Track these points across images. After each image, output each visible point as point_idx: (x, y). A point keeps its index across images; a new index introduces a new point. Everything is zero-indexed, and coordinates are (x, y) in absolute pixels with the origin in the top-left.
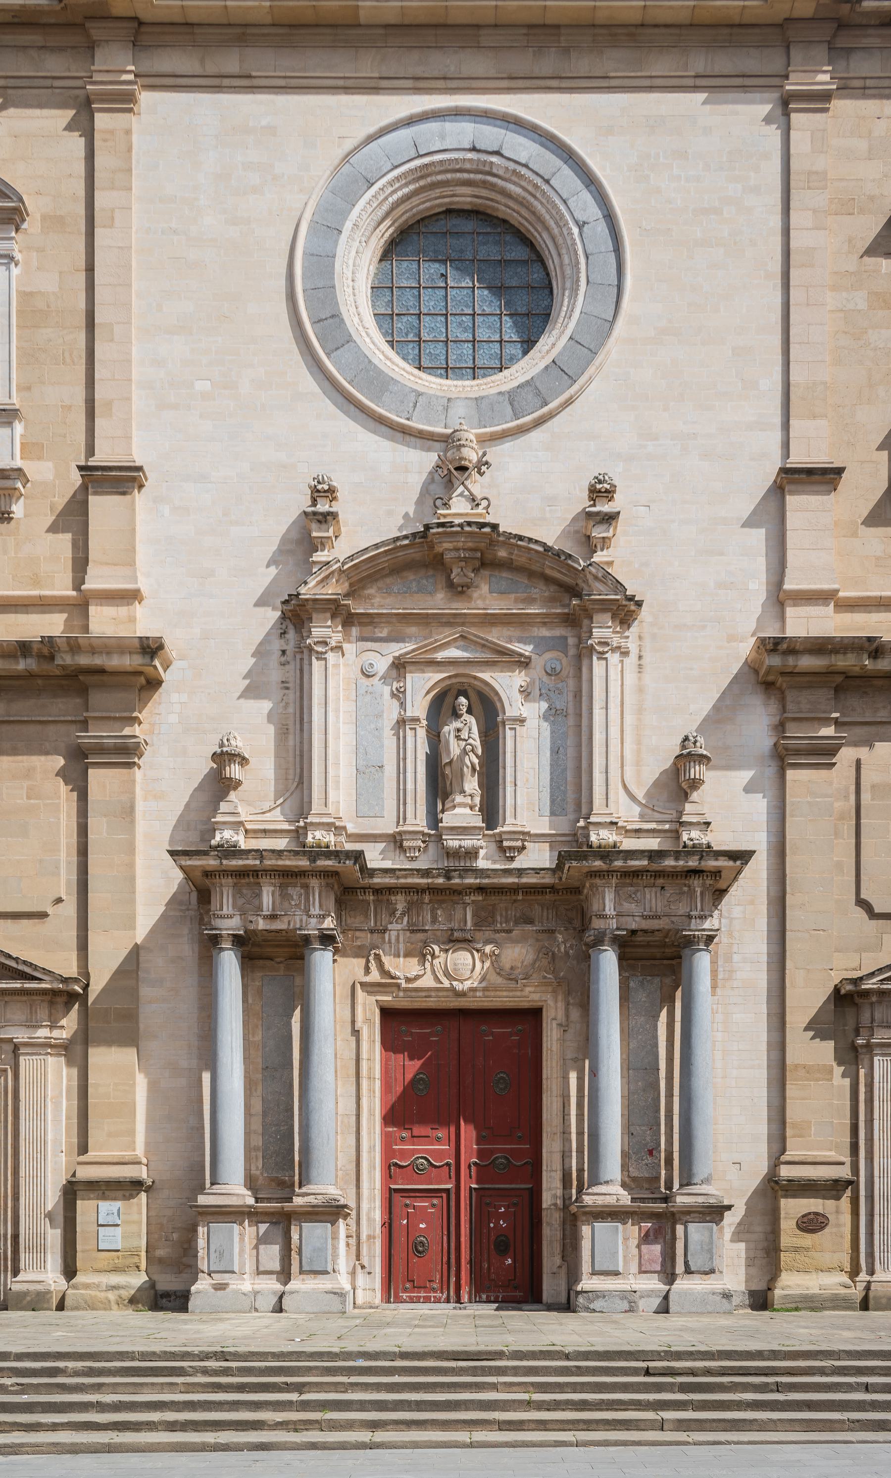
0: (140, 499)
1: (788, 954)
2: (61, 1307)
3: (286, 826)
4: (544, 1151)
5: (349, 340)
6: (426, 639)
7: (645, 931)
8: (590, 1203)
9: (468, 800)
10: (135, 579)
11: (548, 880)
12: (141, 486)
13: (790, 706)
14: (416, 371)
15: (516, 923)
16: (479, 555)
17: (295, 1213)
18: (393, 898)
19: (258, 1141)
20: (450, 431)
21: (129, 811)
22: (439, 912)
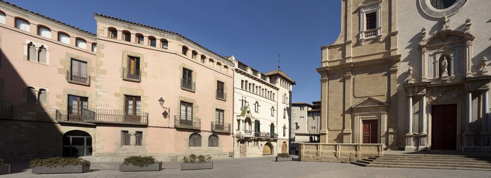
0: (398, 35)
5: (427, 7)
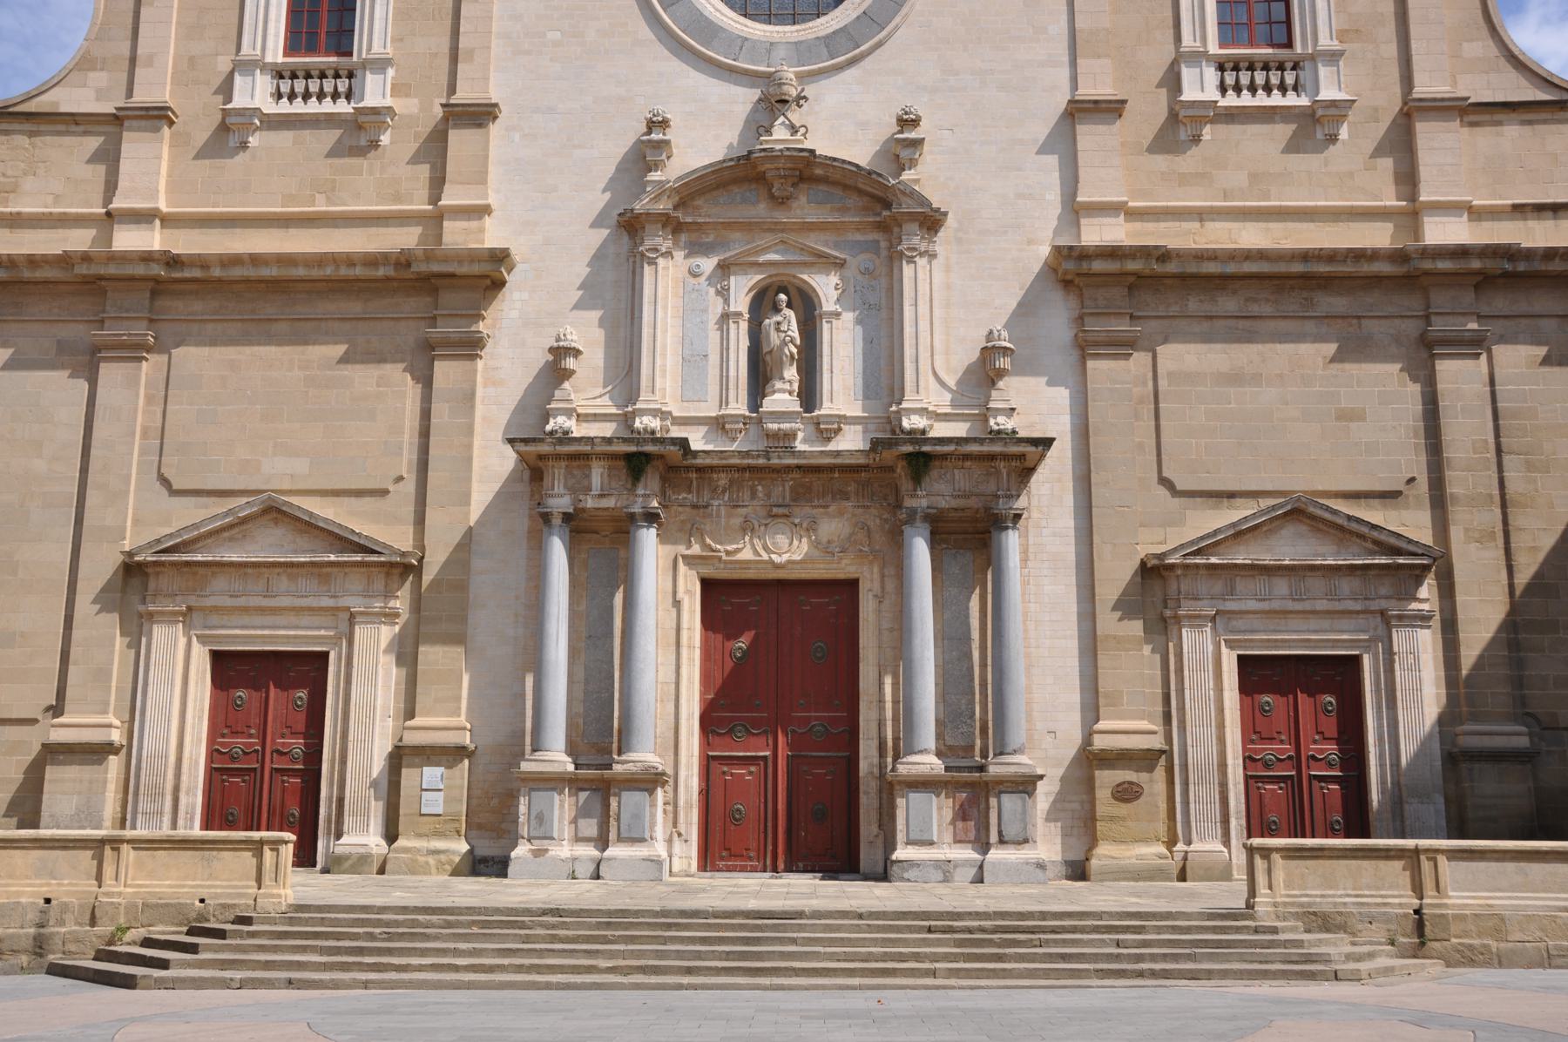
0: (495, 129)
1: (1095, 529)
2: (381, 871)
3: (614, 410)
4: (861, 718)
6: (749, 243)
7: (956, 509)
8: (905, 772)
9: (787, 386)
10: (486, 196)
11: (862, 461)
12: (496, 118)
13: (1087, 302)
14: (742, 19)
15: (834, 499)
16: (798, 173)
17: (614, 780)
18: (715, 476)
19: (579, 708)
20: (773, 70)
21: (470, 397)
22: (760, 488)
